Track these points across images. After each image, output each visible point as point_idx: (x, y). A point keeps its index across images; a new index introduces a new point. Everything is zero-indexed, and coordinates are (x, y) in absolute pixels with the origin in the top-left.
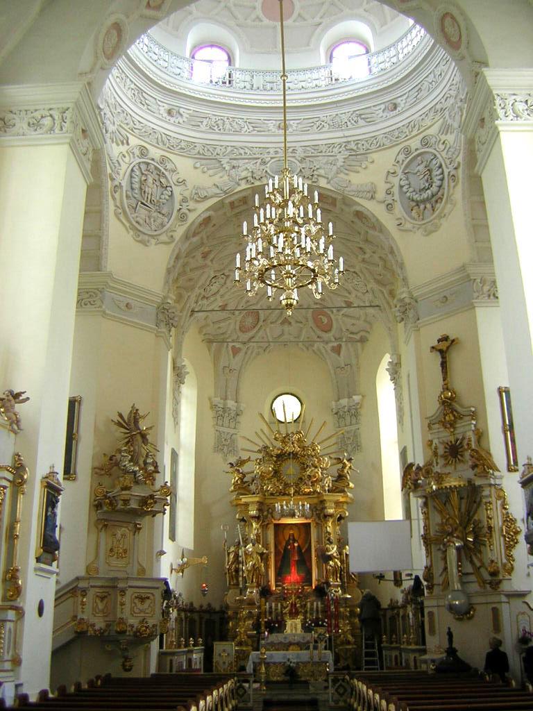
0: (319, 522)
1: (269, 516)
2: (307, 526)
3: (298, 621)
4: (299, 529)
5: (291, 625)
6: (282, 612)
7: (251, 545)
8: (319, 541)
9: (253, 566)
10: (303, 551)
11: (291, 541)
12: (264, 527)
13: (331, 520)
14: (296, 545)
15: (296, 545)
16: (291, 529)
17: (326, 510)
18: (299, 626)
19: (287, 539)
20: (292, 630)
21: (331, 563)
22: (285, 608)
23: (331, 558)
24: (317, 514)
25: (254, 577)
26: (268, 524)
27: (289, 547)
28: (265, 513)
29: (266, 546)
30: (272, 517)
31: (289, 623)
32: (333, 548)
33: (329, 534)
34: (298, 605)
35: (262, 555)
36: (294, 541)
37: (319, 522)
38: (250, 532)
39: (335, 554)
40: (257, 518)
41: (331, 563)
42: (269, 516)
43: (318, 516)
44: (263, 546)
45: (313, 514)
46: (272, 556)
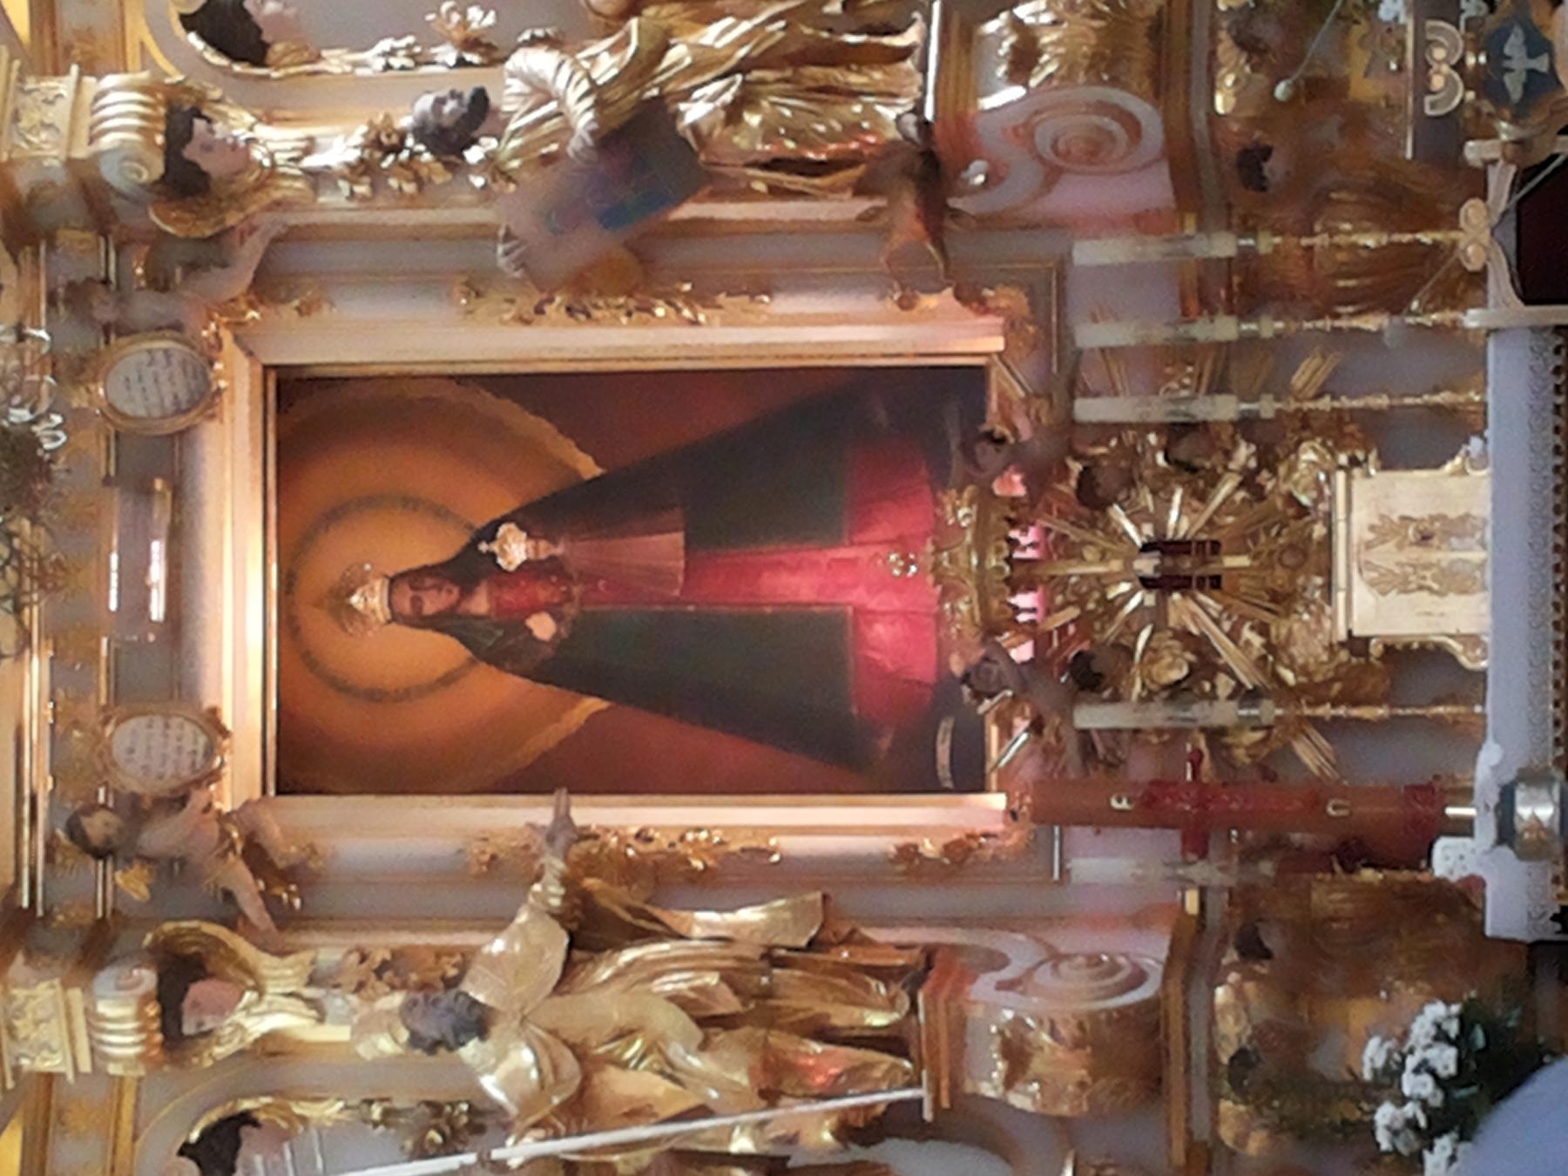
0: (249, 254)
1: (160, 836)
2: (312, 417)
3: (1369, 503)
4: (335, 515)
5: (1382, 585)
6: (1244, 695)
7: (471, 1050)
8: (460, 269)
9: (710, 1023)
10: (588, 467)
11: (480, 603)
12: (295, 898)
13: (237, 124)
14: (515, 549)
15: (515, 549)
16: (337, 600)
17: (111, 173)
18: (1411, 492)
19: (442, 650)
20: (1453, 582)
21: (694, 112)
22: (1205, 663)
23: (638, 140)
24: (159, 283)
25: (842, 1016)
26: (256, 855)
27: (543, 627)
28: (133, 884)
29: (496, 878)
30: (178, 800)
31: (1369, 609)
32: (541, 92)
33: (382, 144)
34: (1178, 521)
35: (590, 931)
36: (470, 566)
37: (249, 254)
38: (337, 1071)
39: (607, 67)
40: (181, 973)
41: (694, 112)
42: (160, 836)
43: (181, 265)
44: (499, 922)
45: (158, 329)
46: (590, 813)
